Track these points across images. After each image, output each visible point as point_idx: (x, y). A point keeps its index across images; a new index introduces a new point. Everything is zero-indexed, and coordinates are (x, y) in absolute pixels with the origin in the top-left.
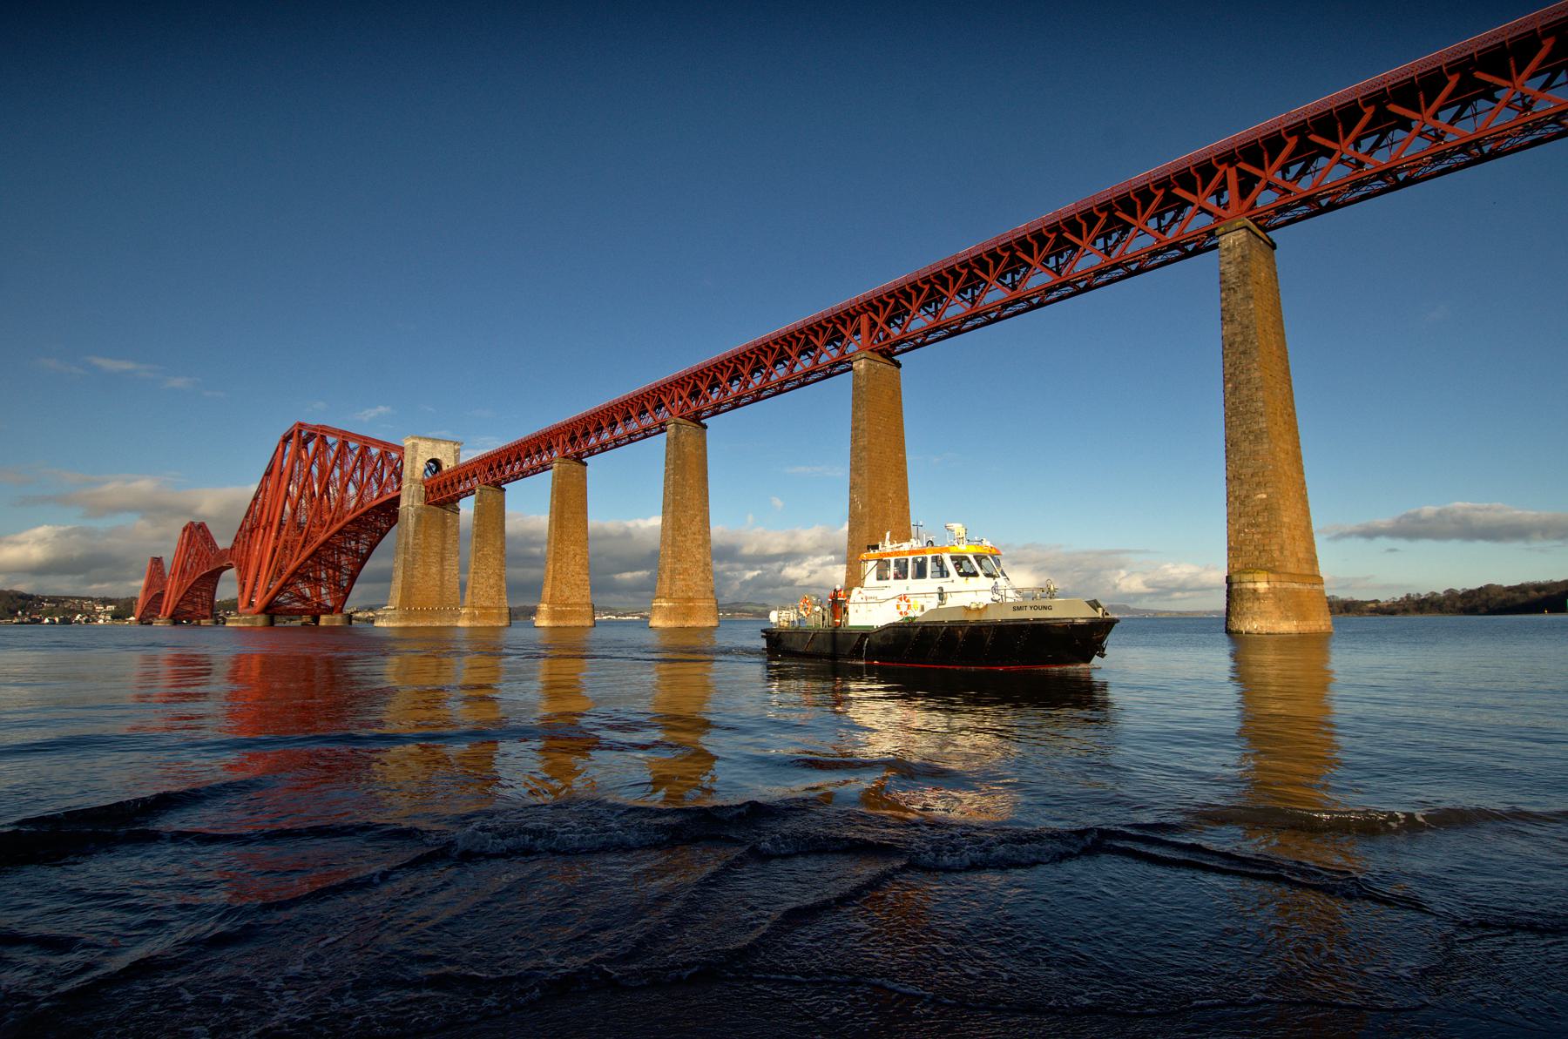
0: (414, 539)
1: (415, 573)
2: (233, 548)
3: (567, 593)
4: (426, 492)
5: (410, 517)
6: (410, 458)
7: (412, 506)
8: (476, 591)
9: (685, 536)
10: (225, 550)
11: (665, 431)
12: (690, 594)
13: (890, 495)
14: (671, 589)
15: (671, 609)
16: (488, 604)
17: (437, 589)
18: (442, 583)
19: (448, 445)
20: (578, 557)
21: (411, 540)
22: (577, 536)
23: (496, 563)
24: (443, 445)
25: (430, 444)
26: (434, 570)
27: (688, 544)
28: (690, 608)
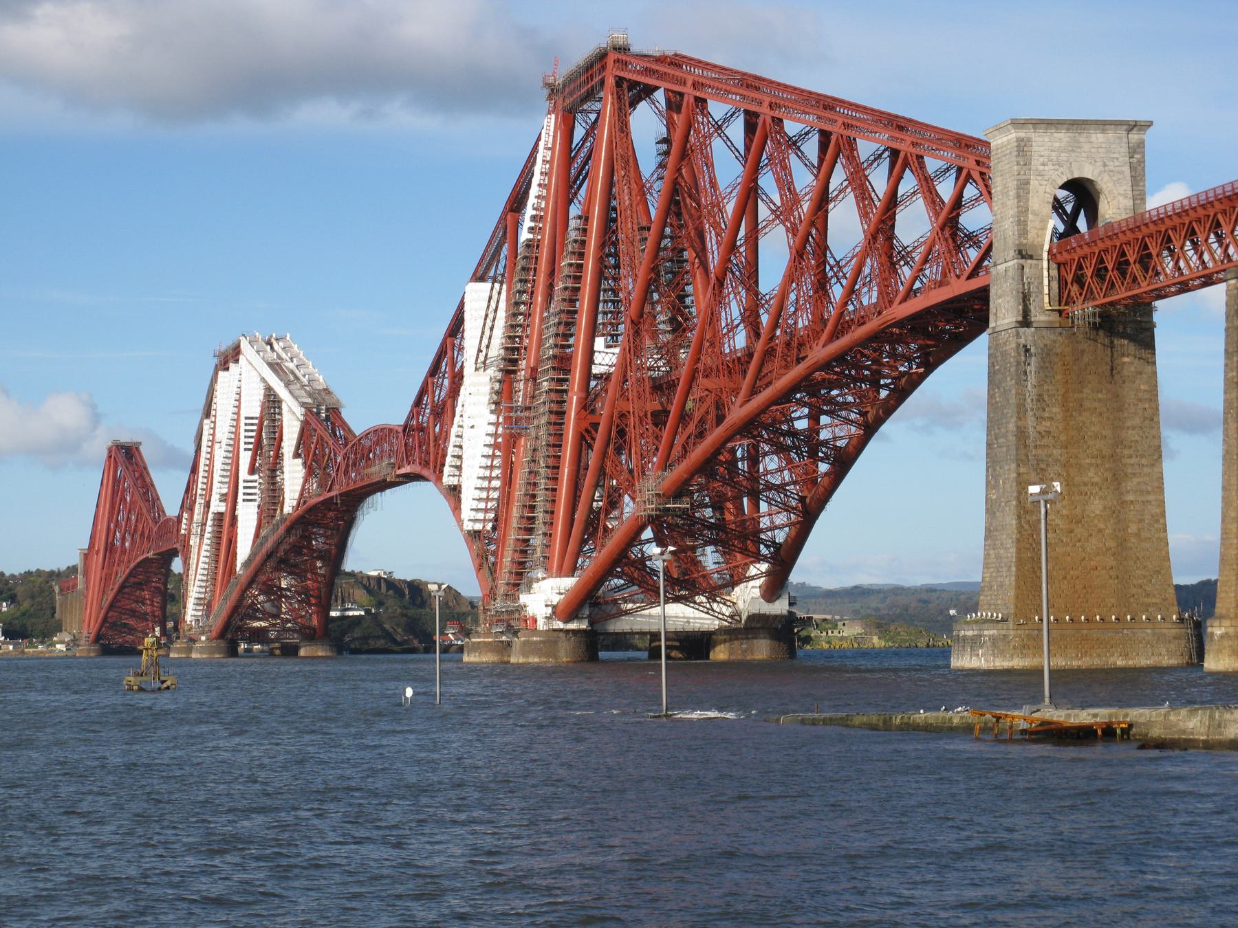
2: (406, 428)
6: (1012, 184)
10: (382, 434)
17: (1111, 562)
18: (1122, 544)
19: (1111, 135)
21: (1030, 421)
24: (1098, 138)
25: (1062, 137)
26: (1096, 506)
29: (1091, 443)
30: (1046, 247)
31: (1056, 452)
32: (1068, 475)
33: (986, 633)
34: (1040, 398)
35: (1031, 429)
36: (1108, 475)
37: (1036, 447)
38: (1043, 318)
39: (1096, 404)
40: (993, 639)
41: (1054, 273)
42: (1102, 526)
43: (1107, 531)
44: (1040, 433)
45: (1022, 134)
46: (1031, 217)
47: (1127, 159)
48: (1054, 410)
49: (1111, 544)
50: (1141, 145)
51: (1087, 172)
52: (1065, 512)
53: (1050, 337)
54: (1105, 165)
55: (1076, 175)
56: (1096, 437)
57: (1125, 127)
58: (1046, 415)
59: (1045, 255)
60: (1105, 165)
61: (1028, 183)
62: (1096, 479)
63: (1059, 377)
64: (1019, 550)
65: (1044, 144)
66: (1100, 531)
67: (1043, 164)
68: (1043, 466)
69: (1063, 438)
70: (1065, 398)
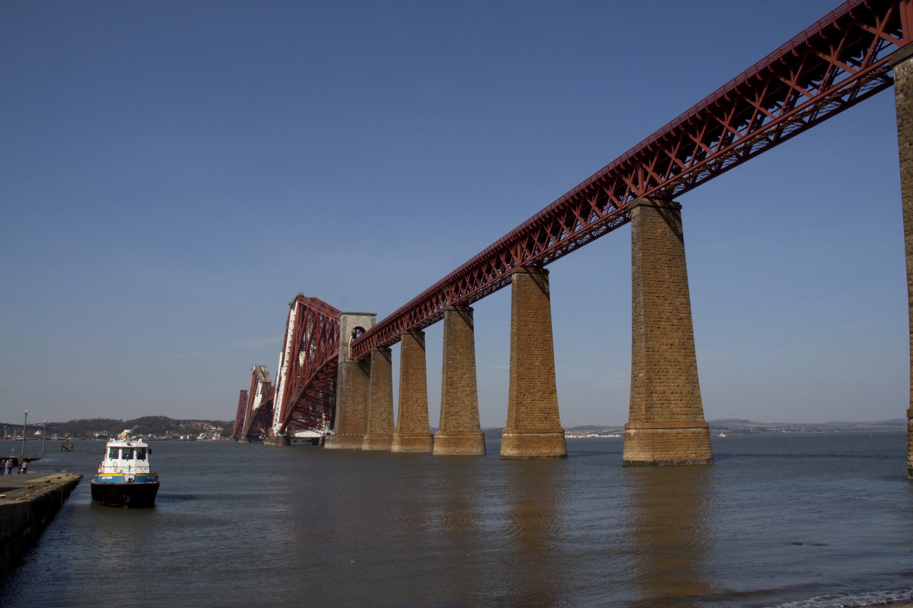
0: (346, 385)
1: (348, 409)
3: (412, 426)
4: (353, 351)
5: (343, 370)
7: (344, 362)
8: (373, 423)
9: (456, 389)
11: (443, 318)
12: (461, 429)
13: (536, 363)
14: (445, 426)
15: (445, 440)
16: (381, 432)
19: (367, 317)
20: (419, 401)
23: (386, 403)
24: (364, 317)
26: (360, 407)
27: (459, 394)
28: (460, 439)
30: (350, 343)
31: (351, 393)
34: (347, 380)
35: (344, 388)
38: (348, 361)
40: (332, 440)
41: (352, 349)
45: (345, 316)
46: (346, 336)
48: (351, 383)
49: (363, 416)
50: (375, 319)
51: (361, 325)
53: (349, 365)
55: (358, 326)
59: (349, 345)
61: (345, 327)
62: (361, 400)
63: (352, 375)
64: (340, 418)
65: (349, 317)
69: (352, 390)
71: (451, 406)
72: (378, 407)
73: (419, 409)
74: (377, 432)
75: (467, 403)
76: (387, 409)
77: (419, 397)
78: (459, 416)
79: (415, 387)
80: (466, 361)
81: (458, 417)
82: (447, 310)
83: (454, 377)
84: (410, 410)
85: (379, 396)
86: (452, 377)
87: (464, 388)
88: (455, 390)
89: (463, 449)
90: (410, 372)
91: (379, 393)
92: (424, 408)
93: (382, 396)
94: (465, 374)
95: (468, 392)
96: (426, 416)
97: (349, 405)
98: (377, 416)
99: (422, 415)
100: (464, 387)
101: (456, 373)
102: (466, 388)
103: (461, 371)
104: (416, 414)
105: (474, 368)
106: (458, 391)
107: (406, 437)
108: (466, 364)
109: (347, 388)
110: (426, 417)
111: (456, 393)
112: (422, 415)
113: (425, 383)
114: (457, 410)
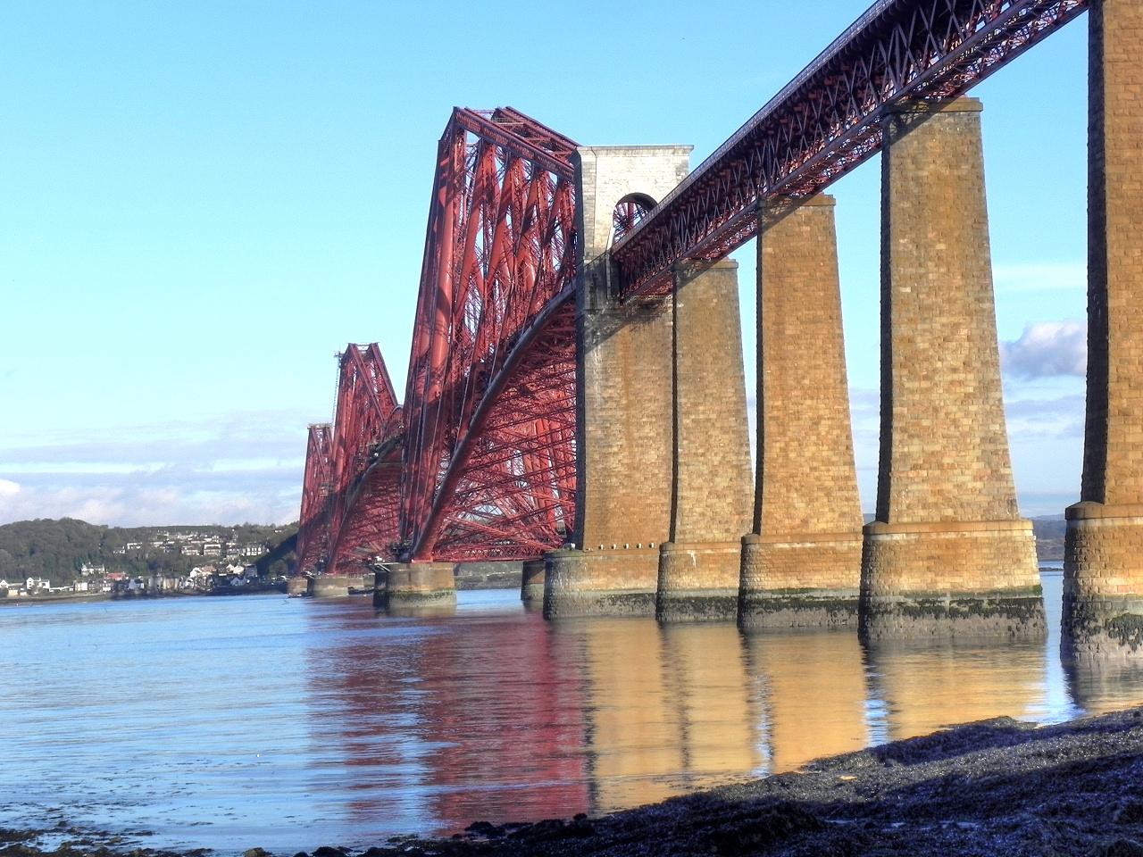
1: (613, 463)
9: (926, 378)
12: (949, 512)
20: (823, 429)
22: (819, 374)
26: (652, 456)
29: (647, 405)
31: (619, 413)
32: (628, 432)
33: (564, 559)
34: (605, 371)
36: (662, 430)
37: (602, 410)
39: (650, 374)
42: (657, 472)
43: (661, 475)
44: (604, 398)
47: (674, 177)
52: (626, 461)
54: (656, 182)
55: (633, 192)
56: (650, 401)
57: (671, 151)
58: (611, 384)
60: (656, 182)
62: (651, 434)
66: (653, 475)
67: (605, 183)
68: (608, 425)
69: (624, 402)
70: (626, 371)
71: (911, 437)
72: (701, 451)
73: (826, 452)
74: (703, 532)
75: (966, 422)
76: (732, 457)
77: (821, 412)
78: (940, 466)
79: (806, 382)
80: (958, 281)
81: (937, 472)
82: (891, 113)
83: (919, 339)
84: (792, 455)
85: (702, 417)
86: (911, 341)
87: (956, 377)
88: (925, 384)
89: (958, 580)
90: (788, 332)
91: (701, 408)
92: (842, 448)
93: (714, 416)
94: (956, 326)
95: (971, 390)
96: (847, 474)
97: (616, 449)
98: (698, 482)
99: (834, 471)
100: (954, 370)
101: (927, 326)
102: (962, 376)
103: (944, 320)
104: (813, 469)
105: (986, 305)
106: (936, 385)
107: (787, 546)
108: (959, 295)
109: (606, 395)
110: (848, 478)
111: (928, 390)
112: (834, 471)
113: (841, 366)
114: (929, 448)
